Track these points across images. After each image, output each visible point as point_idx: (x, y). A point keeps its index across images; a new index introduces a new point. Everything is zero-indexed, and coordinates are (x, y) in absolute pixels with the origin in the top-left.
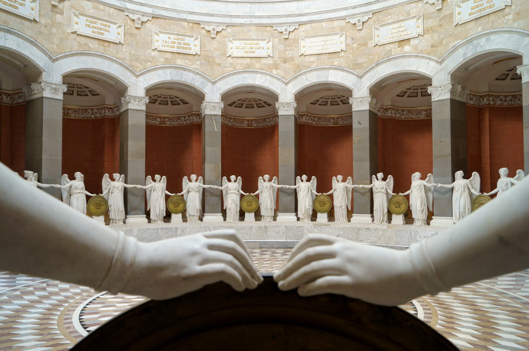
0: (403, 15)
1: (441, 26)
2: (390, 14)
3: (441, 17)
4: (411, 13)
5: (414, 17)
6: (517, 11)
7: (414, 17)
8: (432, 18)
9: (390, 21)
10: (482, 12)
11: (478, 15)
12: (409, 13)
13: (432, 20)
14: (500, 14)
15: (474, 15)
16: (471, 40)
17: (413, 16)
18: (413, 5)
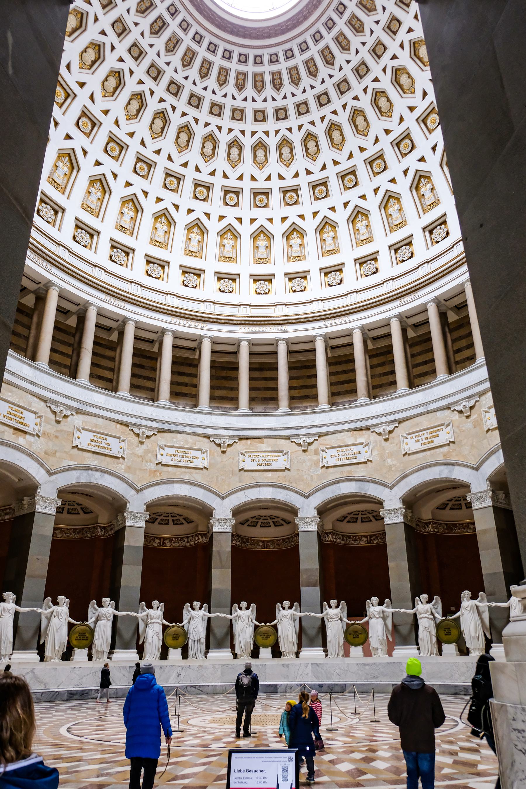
0: (24, 402)
1: (57, 437)
2: (11, 392)
3: (59, 429)
4: (33, 405)
5: (35, 413)
6: (128, 465)
7: (35, 413)
8: (51, 425)
9: (9, 399)
10: (100, 449)
11: (96, 450)
12: (30, 404)
13: (49, 426)
14: (115, 460)
15: (92, 447)
16: (86, 469)
17: (34, 409)
18: (36, 399)
